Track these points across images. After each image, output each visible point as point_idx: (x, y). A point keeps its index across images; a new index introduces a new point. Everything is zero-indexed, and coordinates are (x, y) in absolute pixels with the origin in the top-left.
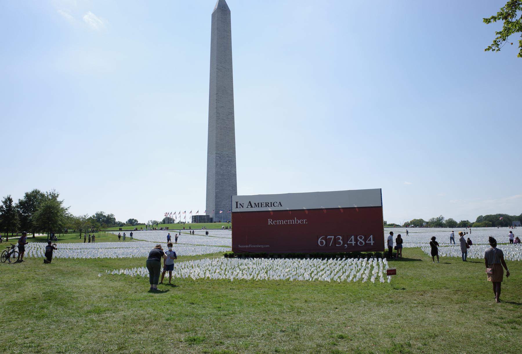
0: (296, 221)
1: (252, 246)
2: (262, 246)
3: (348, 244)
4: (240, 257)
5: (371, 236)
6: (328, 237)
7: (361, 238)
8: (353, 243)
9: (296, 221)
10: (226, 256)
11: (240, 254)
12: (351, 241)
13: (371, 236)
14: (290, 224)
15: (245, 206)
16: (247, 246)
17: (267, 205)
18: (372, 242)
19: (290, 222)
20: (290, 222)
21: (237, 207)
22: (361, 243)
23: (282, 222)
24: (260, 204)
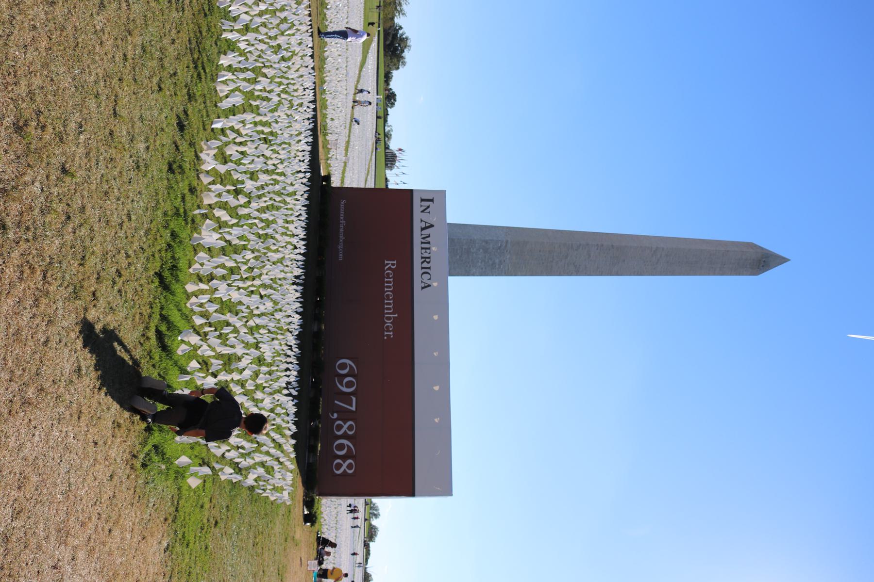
2: (341, 247)
9: (390, 315)
15: (424, 216)
17: (425, 259)
19: (389, 304)
20: (389, 304)
23: (390, 287)
24: (427, 246)
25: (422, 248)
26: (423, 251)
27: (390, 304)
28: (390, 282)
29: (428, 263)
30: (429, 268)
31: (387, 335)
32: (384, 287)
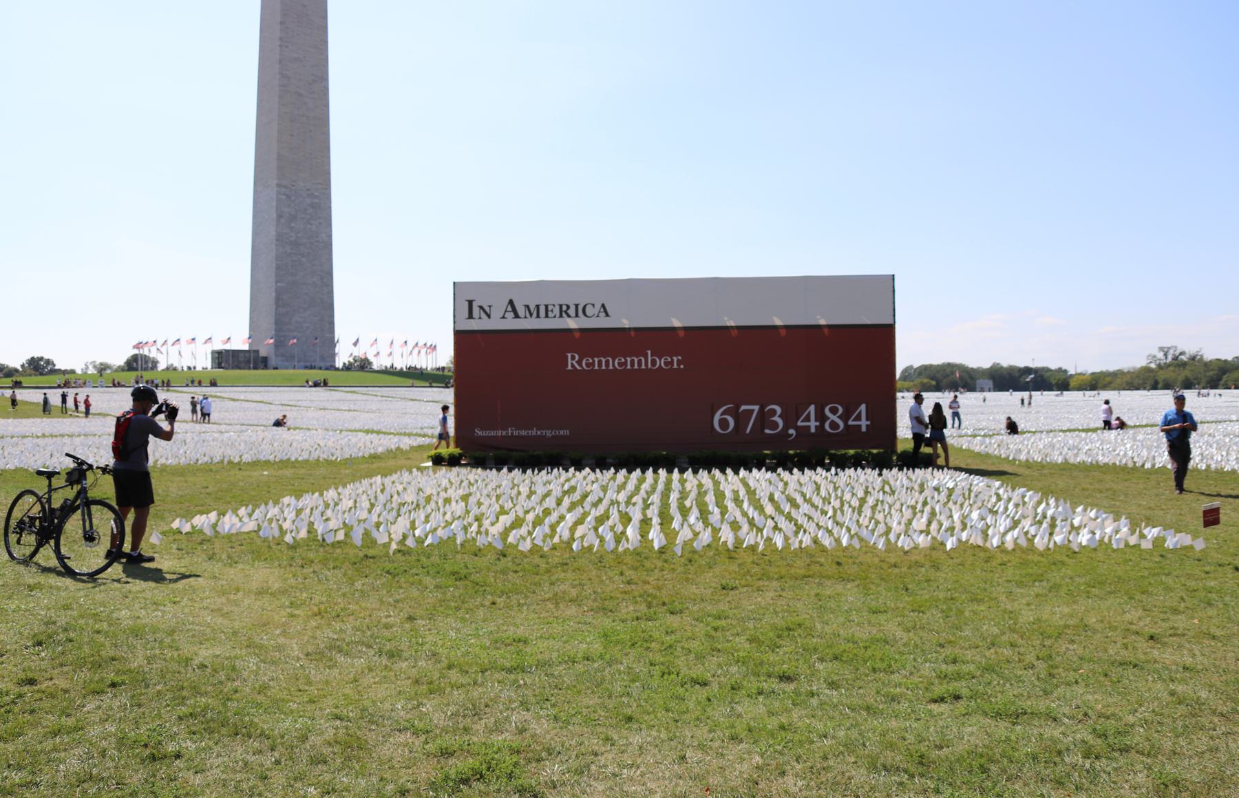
0: (649, 361)
1: (516, 433)
2: (548, 433)
3: (797, 428)
4: (480, 462)
5: (863, 407)
6: (743, 408)
7: (834, 411)
8: (813, 424)
9: (649, 361)
10: (438, 461)
11: (478, 454)
12: (808, 419)
13: (863, 407)
15: (497, 313)
16: (499, 433)
17: (563, 311)
18: (864, 423)
21: (471, 316)
22: (834, 425)
23: (607, 362)
24: (542, 310)
25: (547, 316)
26: (550, 314)
27: (632, 362)
28: (600, 363)
29: (568, 307)
30: (577, 306)
31: (679, 364)
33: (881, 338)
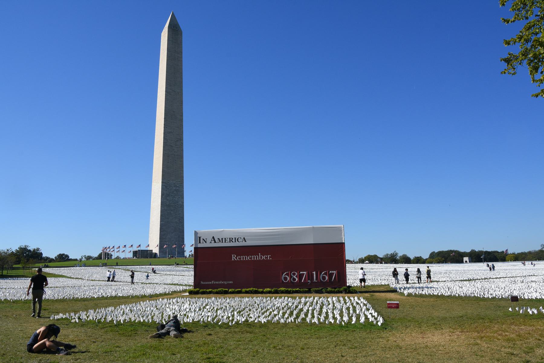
0: (260, 257)
1: (215, 283)
2: (226, 283)
9: (260, 257)
14: (254, 260)
19: (254, 258)
20: (254, 258)
32: (246, 261)
33: (340, 247)
